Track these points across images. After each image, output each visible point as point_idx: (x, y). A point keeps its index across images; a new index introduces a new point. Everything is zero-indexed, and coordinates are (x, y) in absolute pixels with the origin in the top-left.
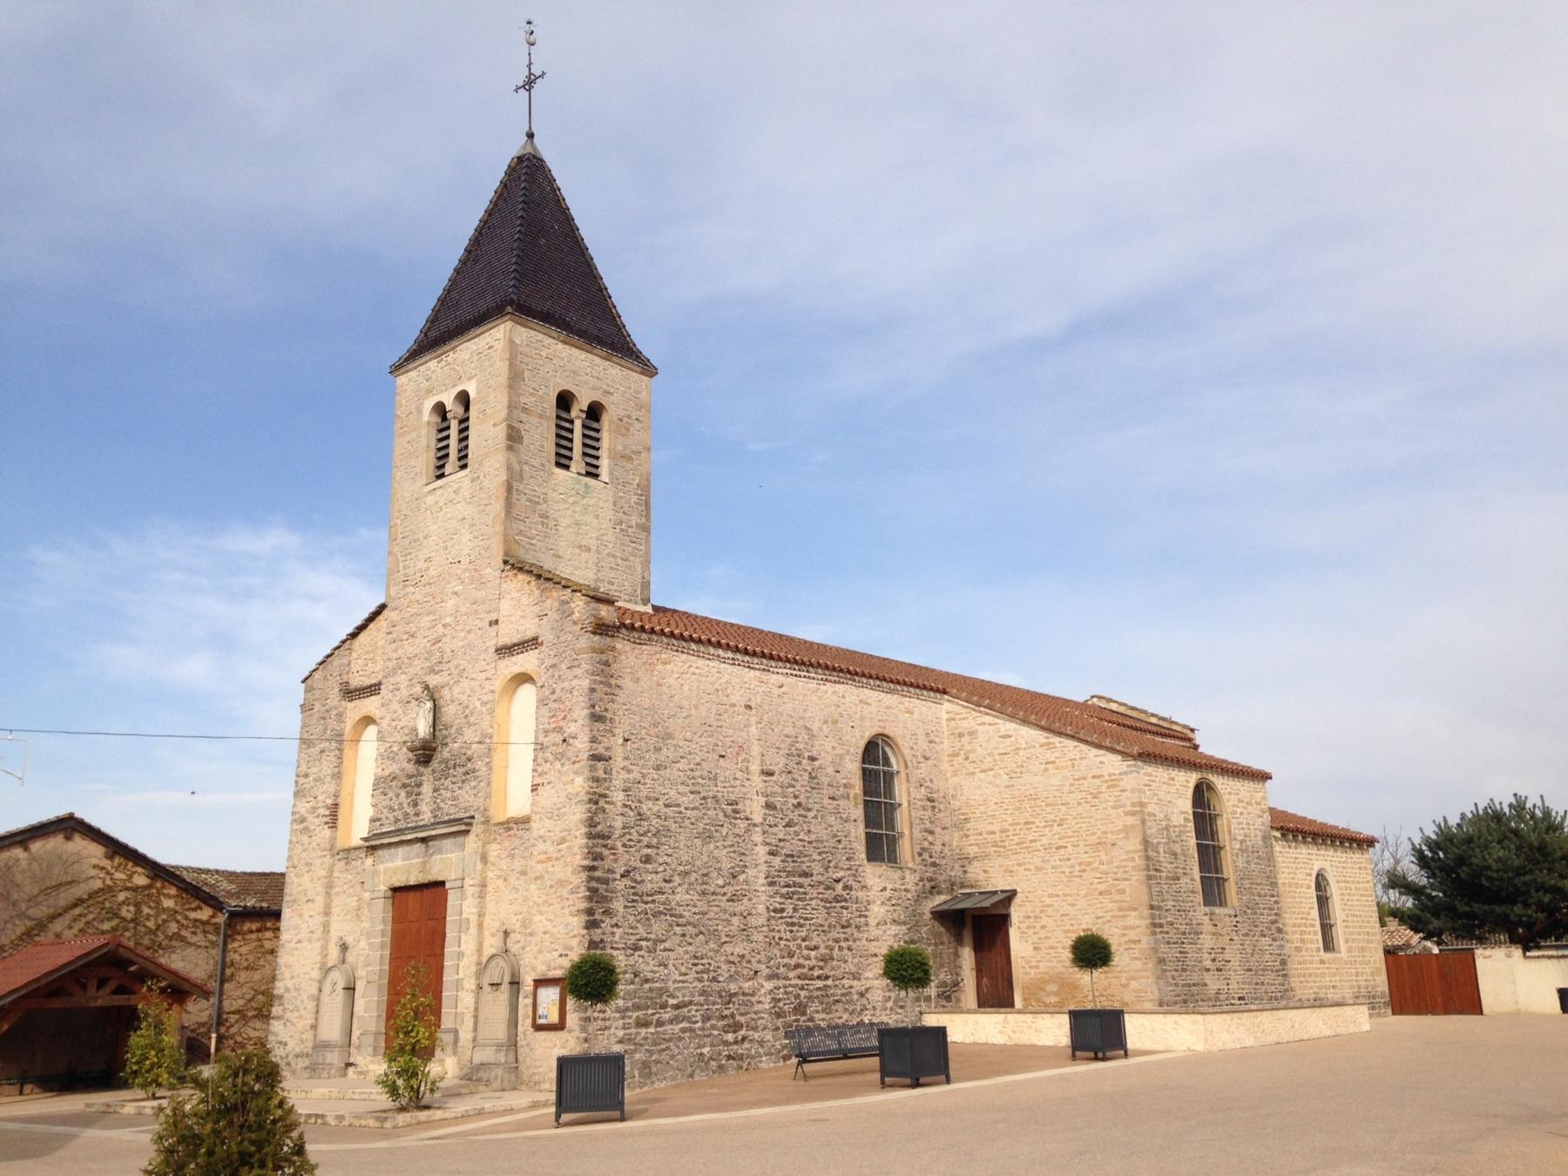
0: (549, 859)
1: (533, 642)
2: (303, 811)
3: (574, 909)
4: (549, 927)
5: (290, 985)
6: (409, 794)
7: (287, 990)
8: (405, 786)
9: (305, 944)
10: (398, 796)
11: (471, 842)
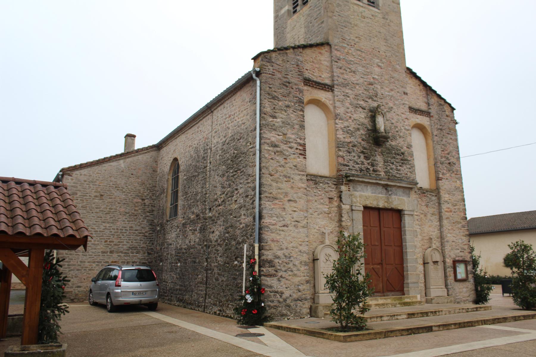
0: (451, 211)
1: (427, 114)
2: (273, 139)
3: (464, 234)
4: (454, 239)
5: (280, 253)
6: (367, 158)
7: (278, 257)
8: (362, 152)
9: (290, 228)
10: (359, 157)
11: (413, 196)
